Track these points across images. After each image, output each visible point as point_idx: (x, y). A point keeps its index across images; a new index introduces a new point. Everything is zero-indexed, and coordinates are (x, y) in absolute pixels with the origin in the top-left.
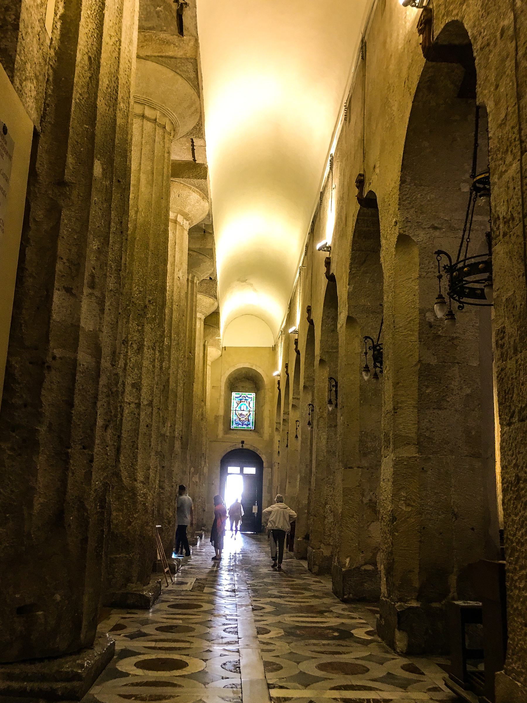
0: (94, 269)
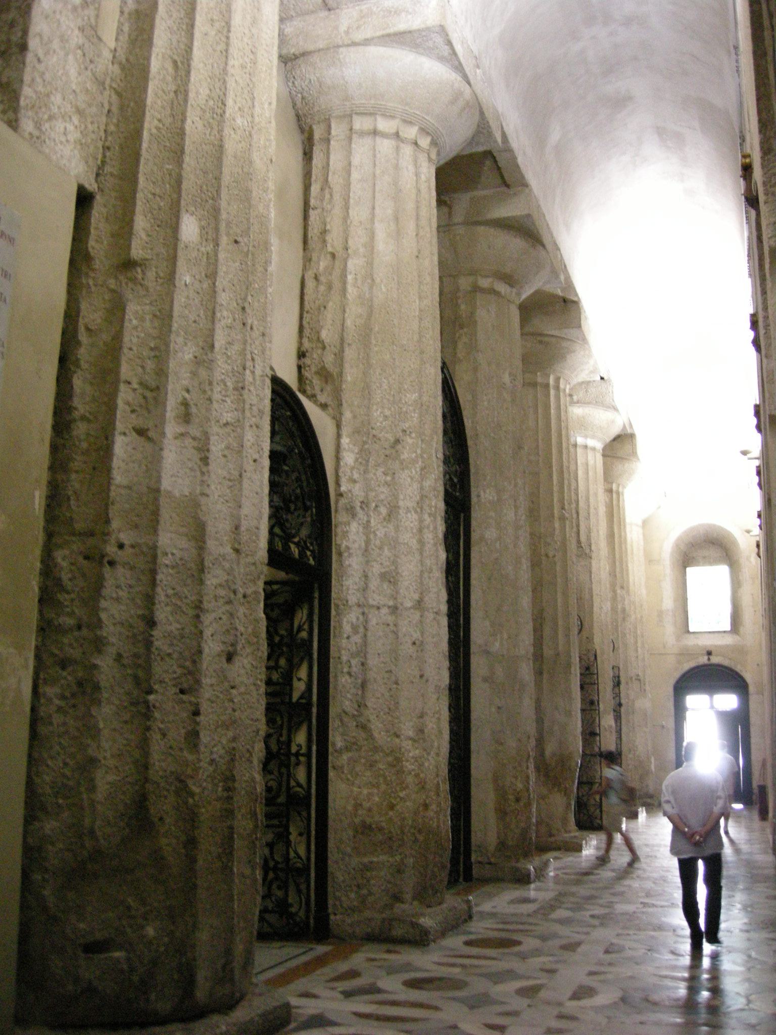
0: (188, 391)
